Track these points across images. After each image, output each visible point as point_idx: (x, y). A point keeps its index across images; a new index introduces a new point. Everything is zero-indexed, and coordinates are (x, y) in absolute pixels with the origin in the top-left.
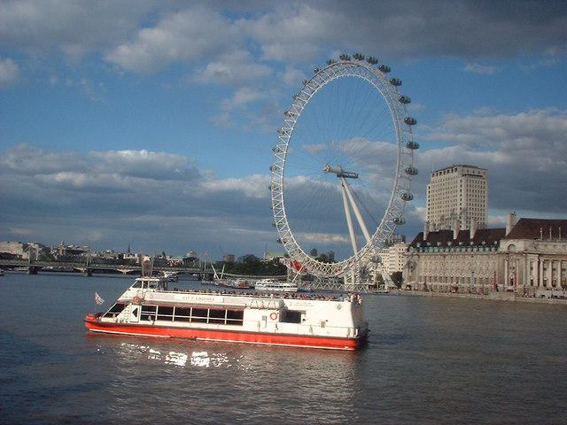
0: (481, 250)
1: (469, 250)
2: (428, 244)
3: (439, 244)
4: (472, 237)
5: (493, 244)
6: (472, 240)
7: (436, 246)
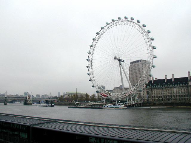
0: (179, 85)
1: (173, 85)
2: (155, 85)
3: (159, 84)
4: (173, 81)
5: (183, 83)
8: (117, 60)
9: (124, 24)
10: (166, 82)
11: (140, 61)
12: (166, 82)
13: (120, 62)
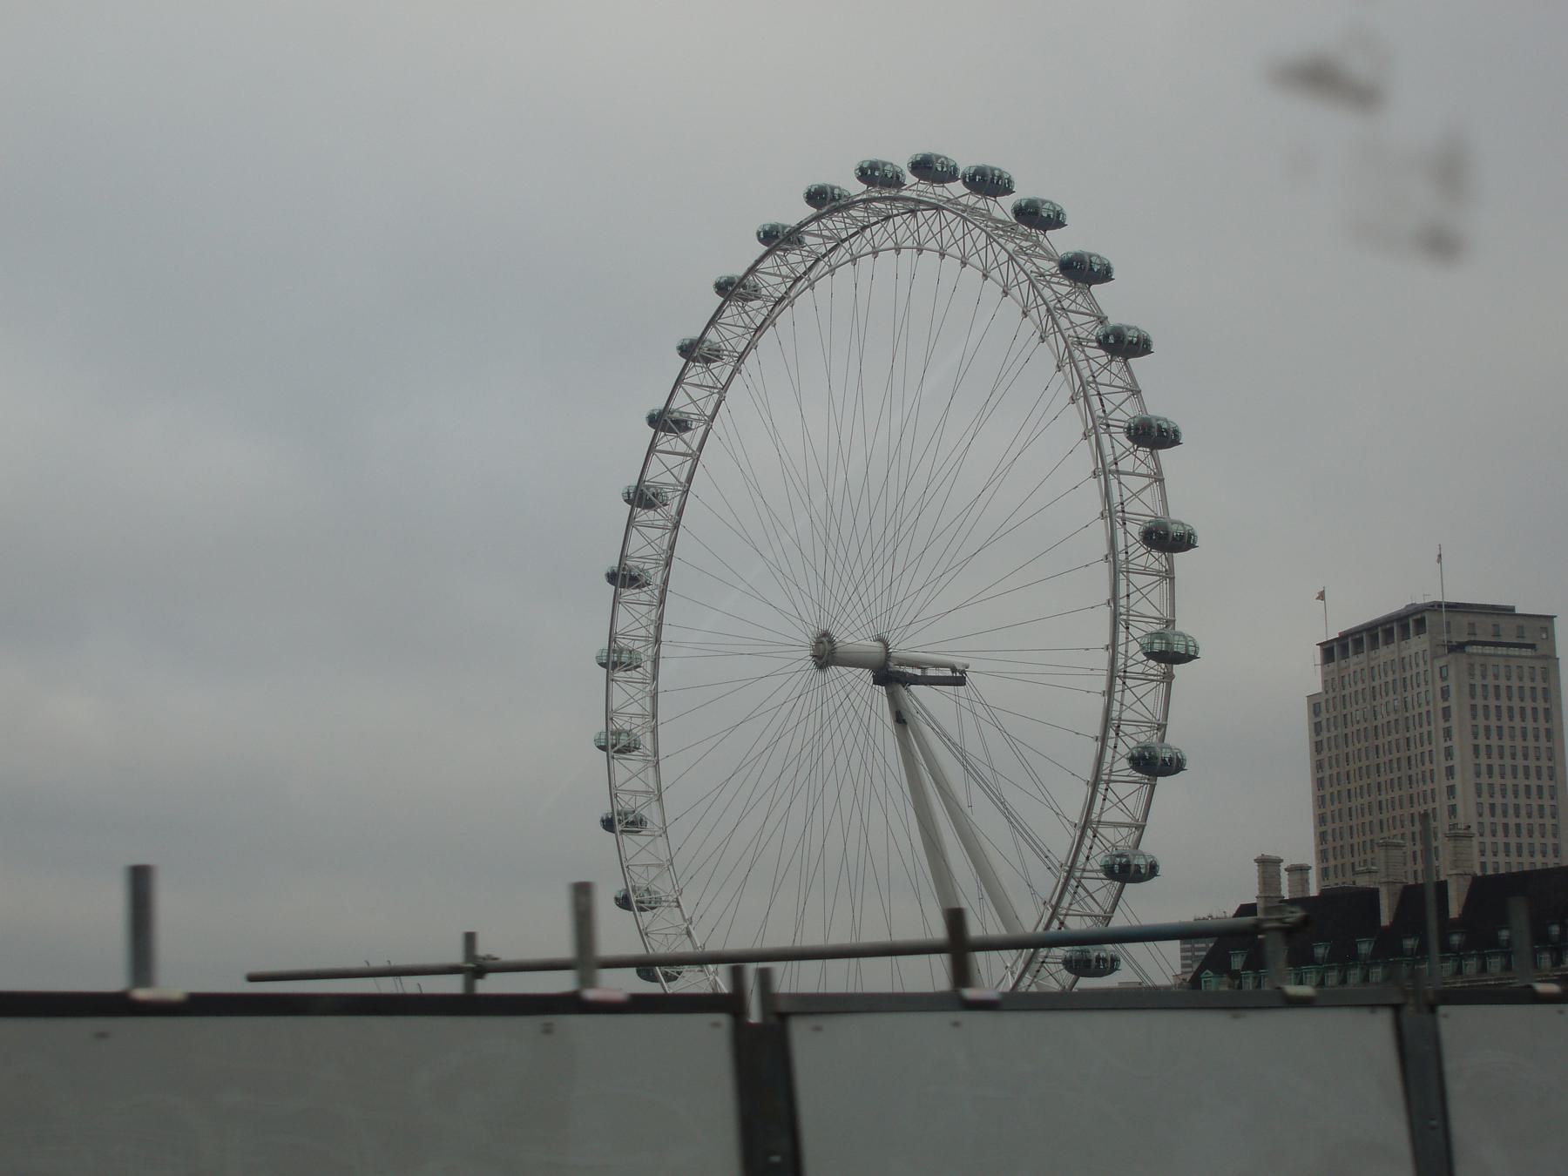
6: (1462, 924)
7: (1311, 960)
8: (867, 675)
9: (875, 253)
10: (1385, 919)
11: (1421, 625)
12: (1385, 919)
13: (894, 700)
